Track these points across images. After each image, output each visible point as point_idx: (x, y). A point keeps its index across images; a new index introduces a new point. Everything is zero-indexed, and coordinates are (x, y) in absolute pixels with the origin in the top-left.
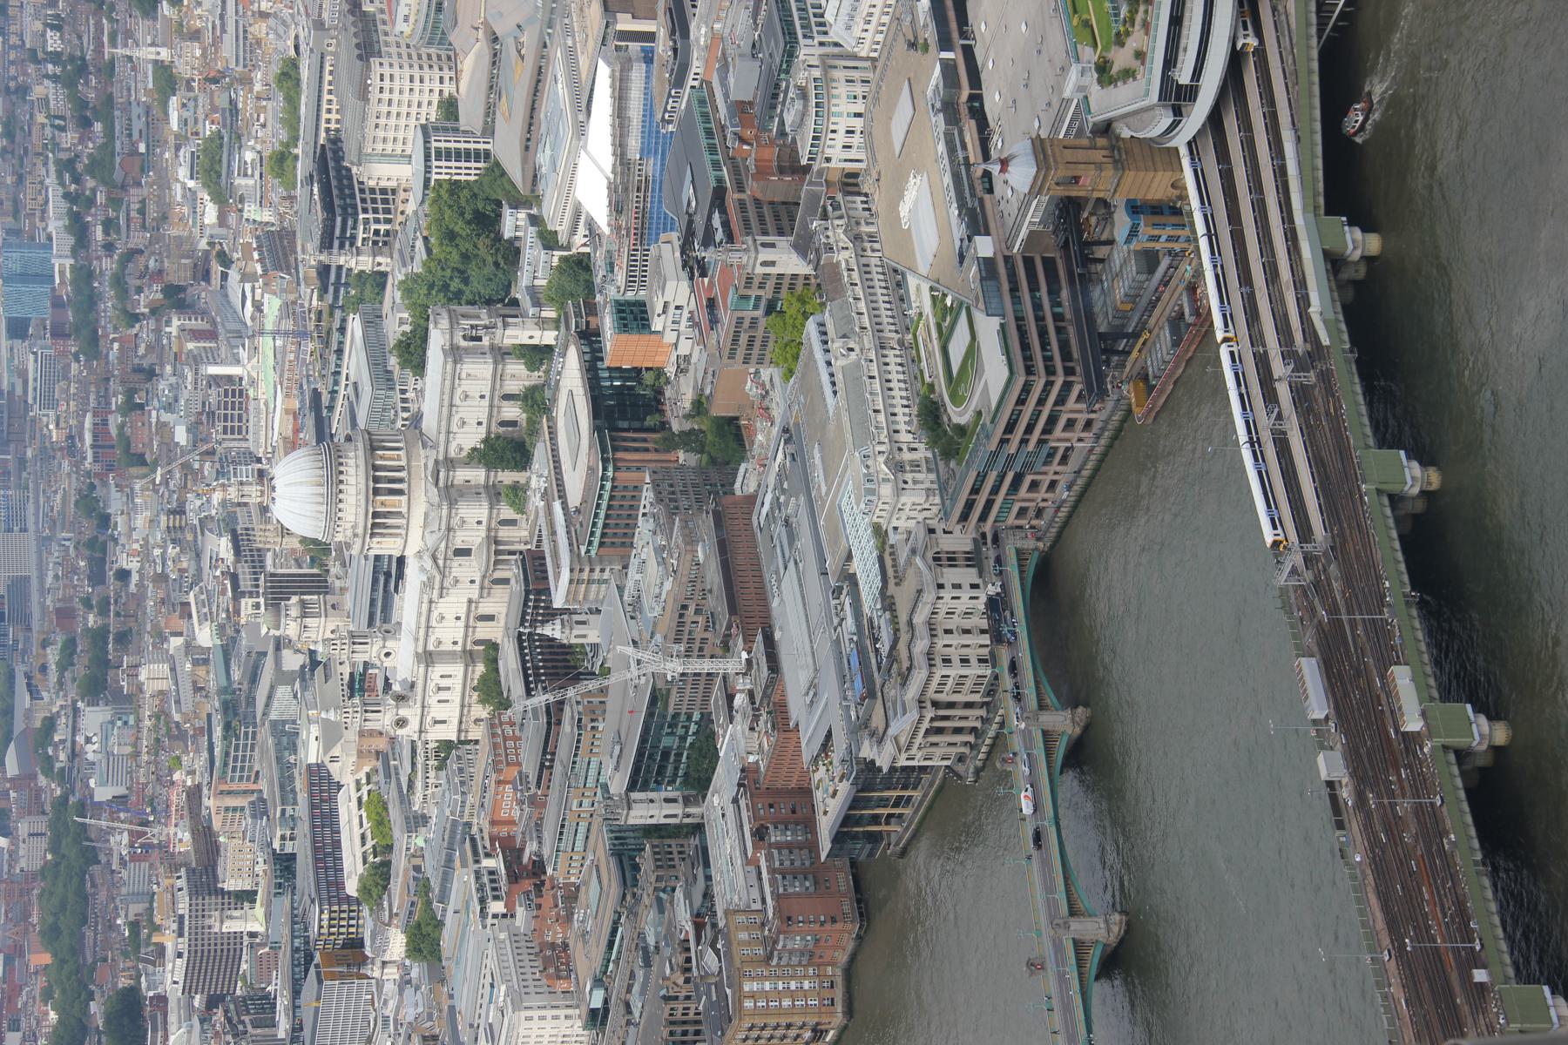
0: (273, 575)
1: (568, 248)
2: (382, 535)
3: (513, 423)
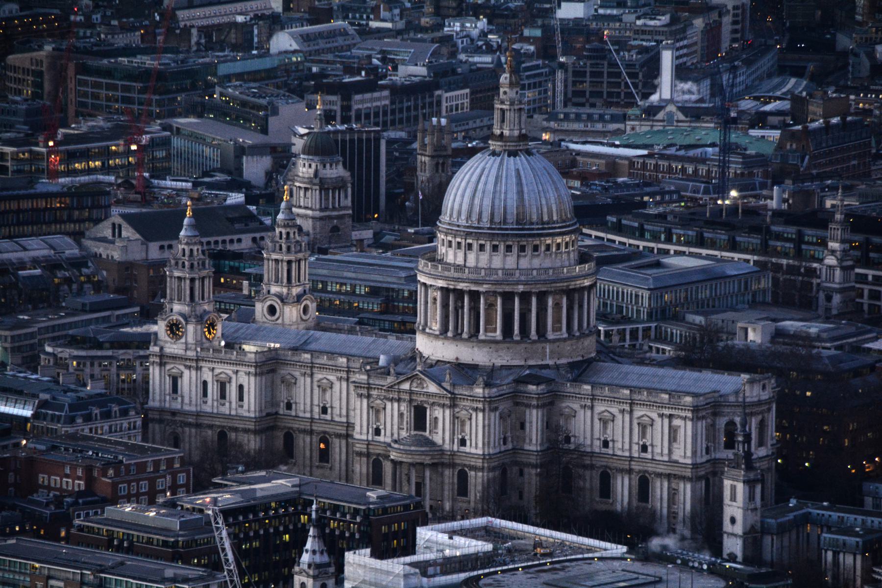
0: (377, 140)
2: (445, 306)
3: (606, 489)
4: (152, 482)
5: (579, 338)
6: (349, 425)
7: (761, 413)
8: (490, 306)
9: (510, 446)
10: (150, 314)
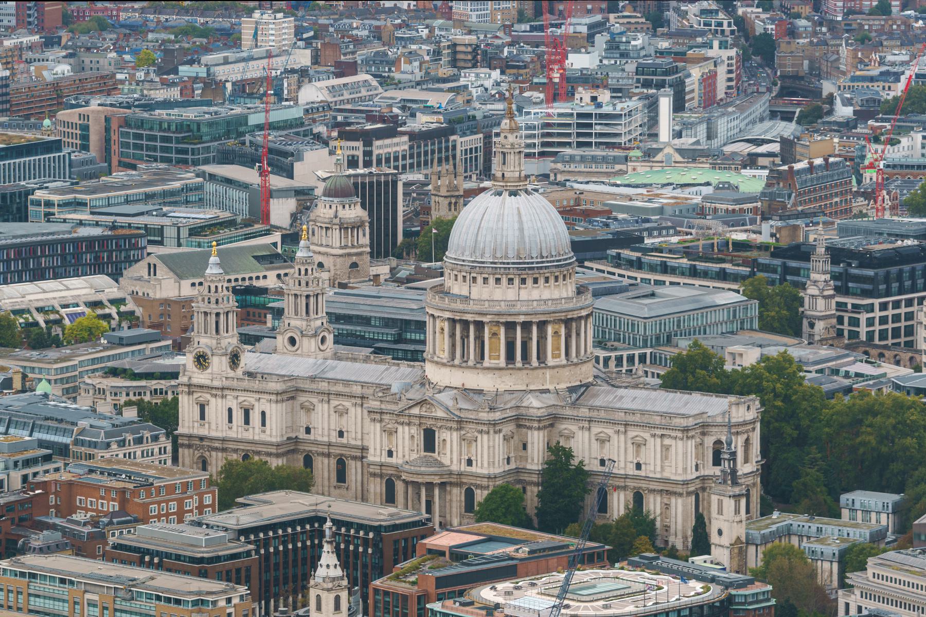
1: (843, 585)
3: (603, 506)
4: (180, 502)
5: (576, 364)
6: (364, 449)
7: (747, 432)
9: (513, 466)
10: (179, 347)
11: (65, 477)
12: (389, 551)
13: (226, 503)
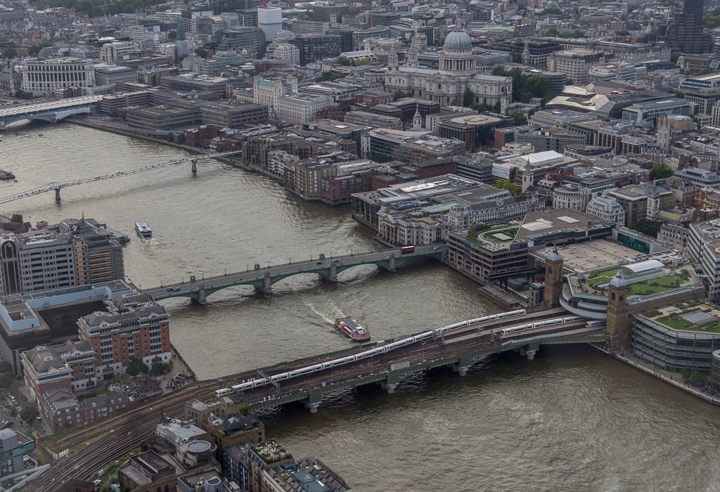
3: (477, 101)
8: (454, 63)
10: (385, 66)
11: (360, 94)
12: (430, 110)
13: (395, 100)
